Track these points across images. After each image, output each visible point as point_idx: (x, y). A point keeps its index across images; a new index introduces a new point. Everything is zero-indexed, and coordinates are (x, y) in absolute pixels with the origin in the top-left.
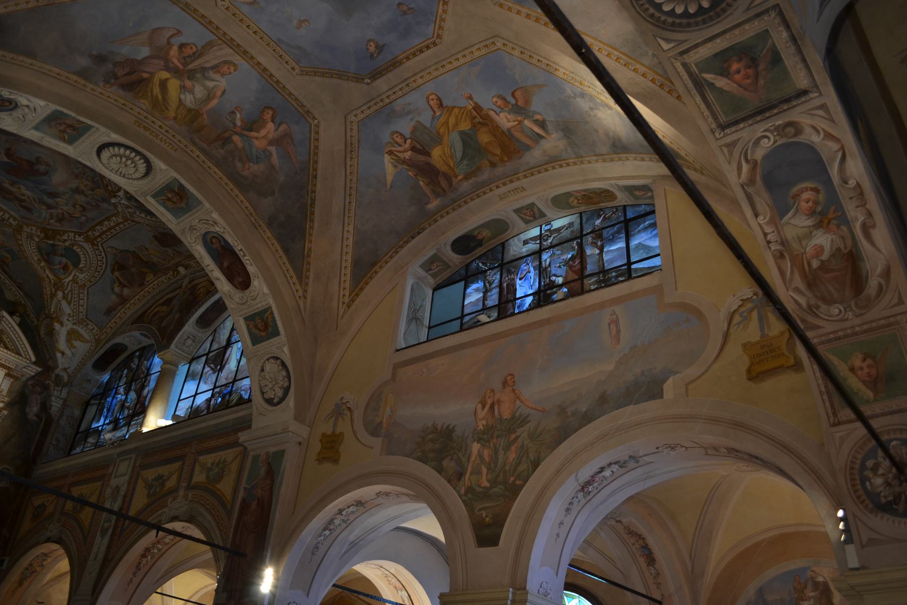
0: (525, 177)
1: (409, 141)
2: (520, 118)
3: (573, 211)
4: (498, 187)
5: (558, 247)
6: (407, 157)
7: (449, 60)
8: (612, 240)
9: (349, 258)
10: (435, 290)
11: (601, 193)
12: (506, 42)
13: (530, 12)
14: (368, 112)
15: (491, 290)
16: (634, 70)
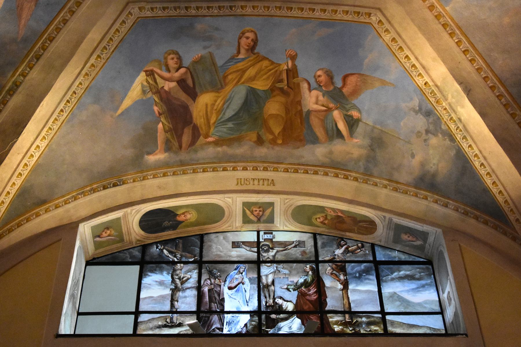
0: (286, 171)
1: (182, 70)
2: (331, 105)
3: (306, 228)
4: (245, 169)
5: (285, 265)
6: (166, 88)
7: (302, 6)
8: (360, 277)
9: (19, 182)
10: (89, 263)
11: (360, 222)
12: (384, 20)
13: (436, 4)
14: (160, 13)
15: (184, 290)
16: (511, 115)
